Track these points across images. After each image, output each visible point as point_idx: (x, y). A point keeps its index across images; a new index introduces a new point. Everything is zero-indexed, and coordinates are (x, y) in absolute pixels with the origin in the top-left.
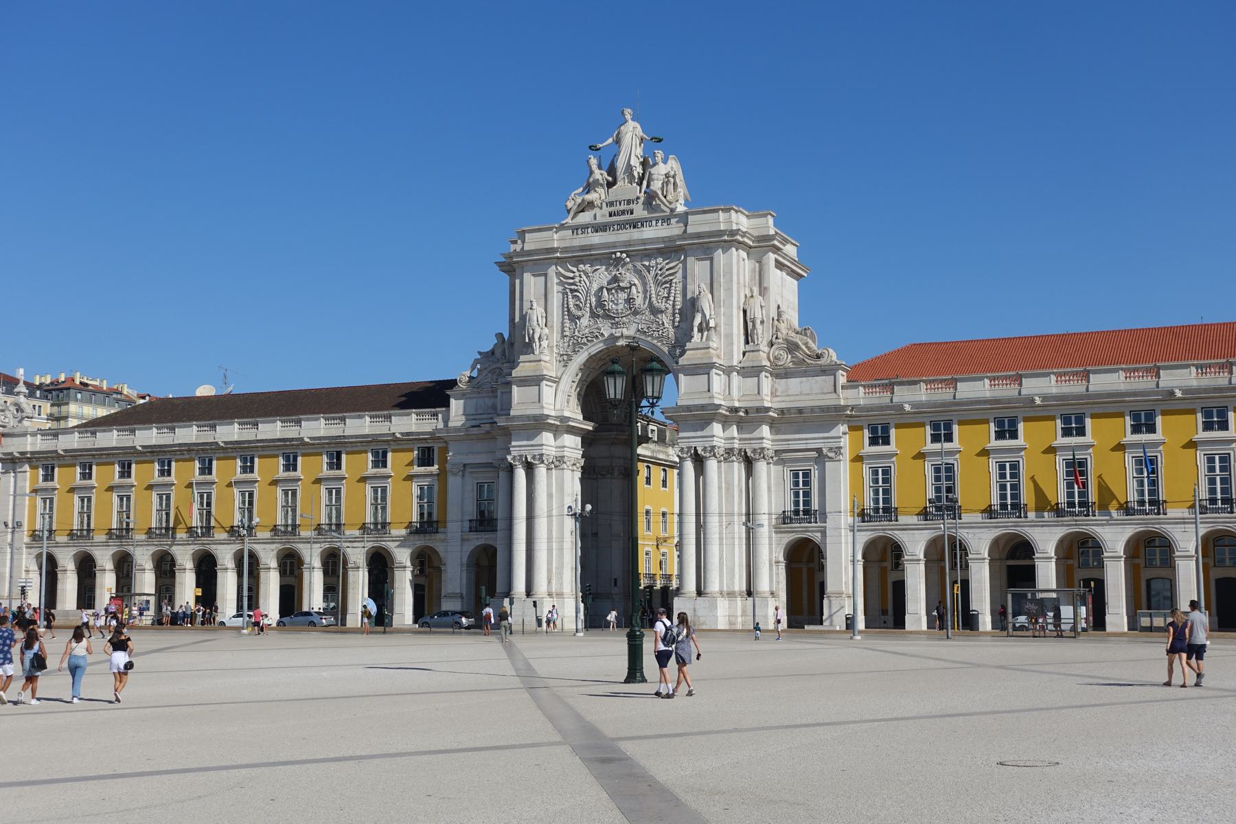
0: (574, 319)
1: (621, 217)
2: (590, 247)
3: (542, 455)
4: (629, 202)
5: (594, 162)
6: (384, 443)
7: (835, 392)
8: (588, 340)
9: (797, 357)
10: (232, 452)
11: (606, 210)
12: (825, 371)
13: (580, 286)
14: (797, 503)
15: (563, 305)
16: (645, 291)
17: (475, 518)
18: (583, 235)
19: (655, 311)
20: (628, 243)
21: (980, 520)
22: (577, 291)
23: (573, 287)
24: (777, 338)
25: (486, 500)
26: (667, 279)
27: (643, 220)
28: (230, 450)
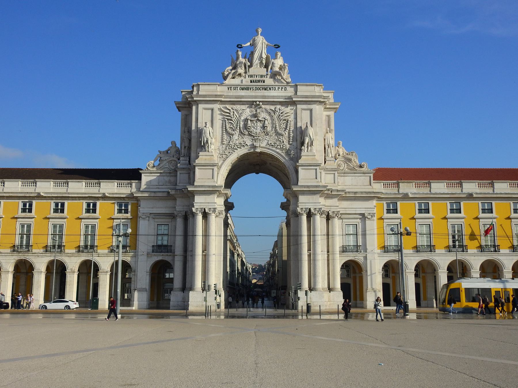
0: (230, 135)
2: (242, 97)
3: (215, 209)
4: (262, 76)
5: (240, 53)
7: (370, 185)
8: (238, 147)
9: (350, 166)
11: (248, 79)
13: (233, 117)
15: (222, 127)
16: (273, 124)
17: (156, 245)
19: (278, 134)
20: (264, 97)
21: (444, 252)
22: (231, 120)
23: (229, 118)
24: (339, 155)
27: (270, 87)
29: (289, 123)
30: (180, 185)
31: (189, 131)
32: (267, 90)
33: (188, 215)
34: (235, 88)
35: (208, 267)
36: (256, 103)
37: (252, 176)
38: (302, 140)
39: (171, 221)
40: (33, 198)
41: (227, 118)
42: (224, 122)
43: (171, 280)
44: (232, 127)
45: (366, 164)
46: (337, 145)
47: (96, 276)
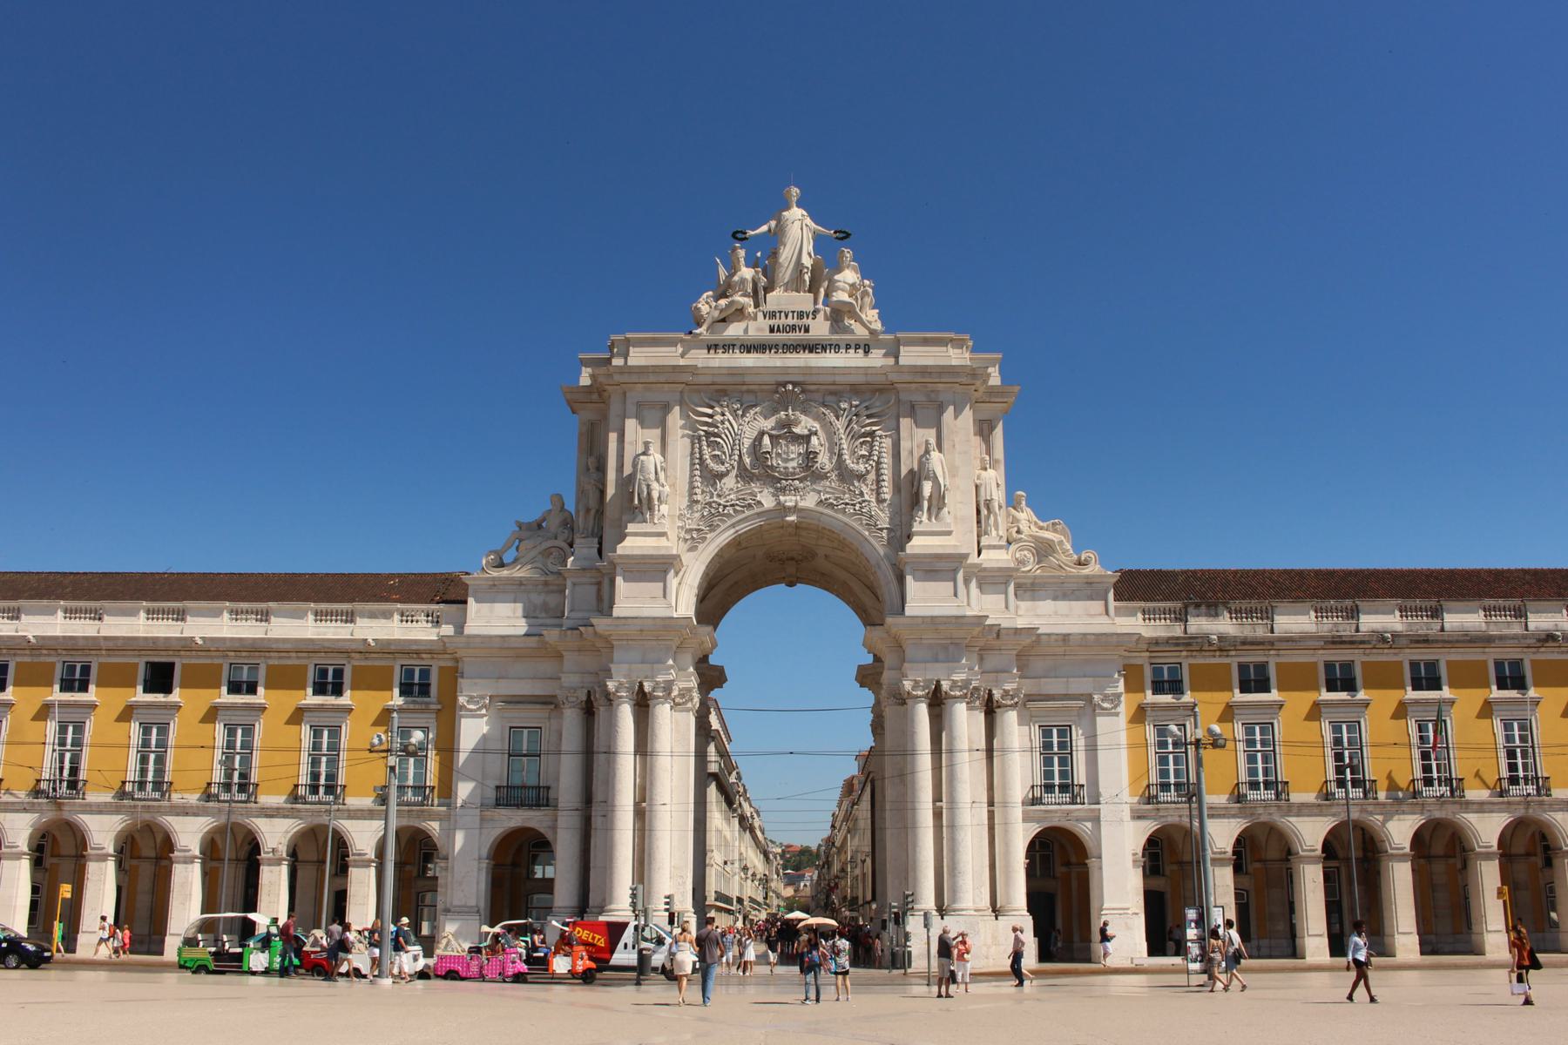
1: (790, 334)
4: (801, 315)
6: (341, 655)
8: (735, 511)
10: (49, 655)
12: (1091, 583)
14: (1048, 775)
15: (692, 454)
17: (505, 784)
18: (726, 355)
20: (808, 370)
23: (711, 429)
24: (1018, 532)
25: (525, 756)
26: (868, 428)
27: (824, 343)
28: (45, 652)
29: (877, 443)
30: (574, 615)
31: (601, 468)
32: (816, 352)
33: (596, 700)
34: (727, 348)
35: (650, 848)
36: (785, 387)
37: (776, 593)
38: (915, 488)
39: (549, 718)
40: (176, 653)
41: (705, 428)
42: (697, 441)
43: (548, 885)
44: (719, 453)
45: (1093, 557)
46: (1012, 502)
47: (342, 869)
